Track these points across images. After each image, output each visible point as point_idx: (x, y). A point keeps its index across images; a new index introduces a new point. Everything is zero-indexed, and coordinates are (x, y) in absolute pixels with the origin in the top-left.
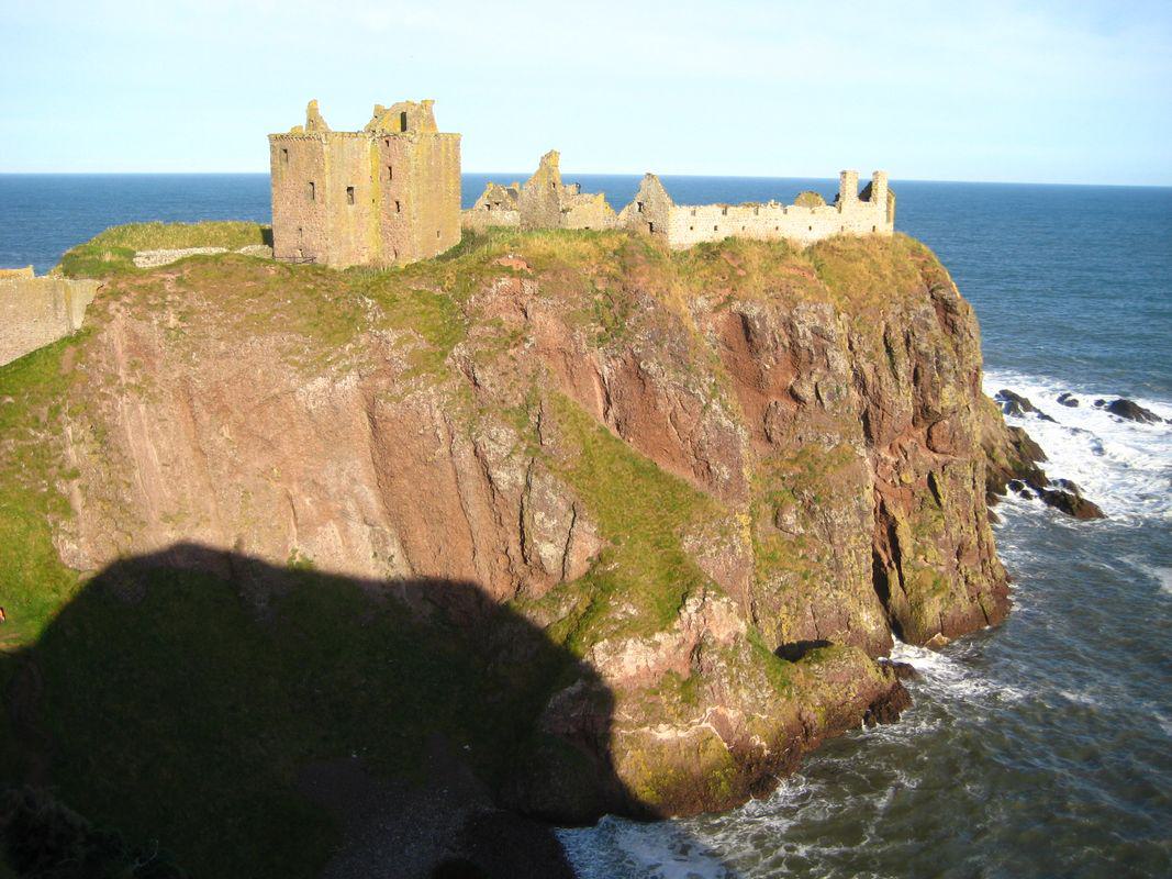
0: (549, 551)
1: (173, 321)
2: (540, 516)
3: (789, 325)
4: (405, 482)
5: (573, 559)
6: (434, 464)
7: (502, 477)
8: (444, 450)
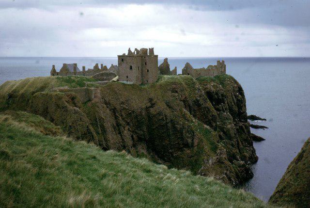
0: (190, 141)
3: (217, 94)
7: (178, 126)
8: (164, 122)
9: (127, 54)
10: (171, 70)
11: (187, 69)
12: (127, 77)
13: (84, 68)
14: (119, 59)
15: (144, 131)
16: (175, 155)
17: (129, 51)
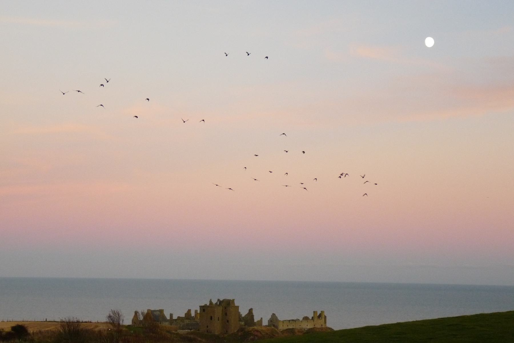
9: (208, 304)
10: (255, 321)
11: (274, 320)
12: (207, 327)
13: (171, 315)
17: (211, 302)
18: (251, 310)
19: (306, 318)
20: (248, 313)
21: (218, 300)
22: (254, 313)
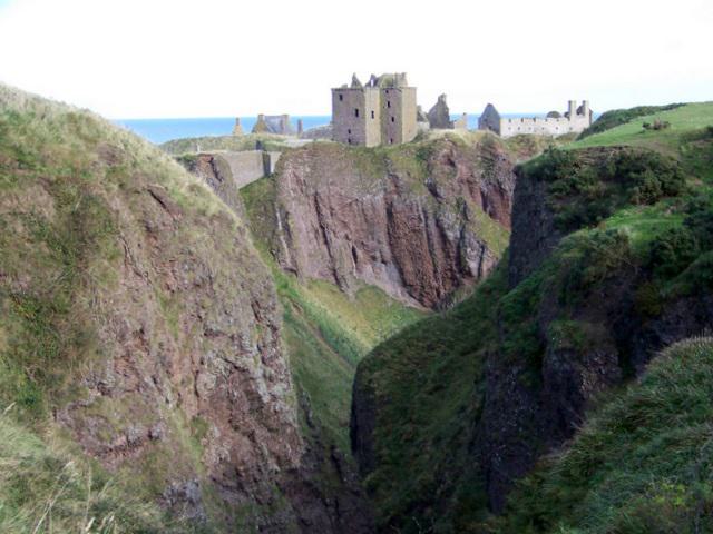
0: (473, 265)
1: (308, 170)
2: (469, 250)
4: (404, 241)
5: (485, 268)
6: (419, 231)
7: (451, 235)
8: (423, 225)
9: (349, 86)
14: (334, 95)
15: (379, 242)
16: (442, 292)
17: (355, 81)
18: (441, 102)
19: (554, 115)
20: (437, 105)
21: (373, 77)
22: (449, 103)
